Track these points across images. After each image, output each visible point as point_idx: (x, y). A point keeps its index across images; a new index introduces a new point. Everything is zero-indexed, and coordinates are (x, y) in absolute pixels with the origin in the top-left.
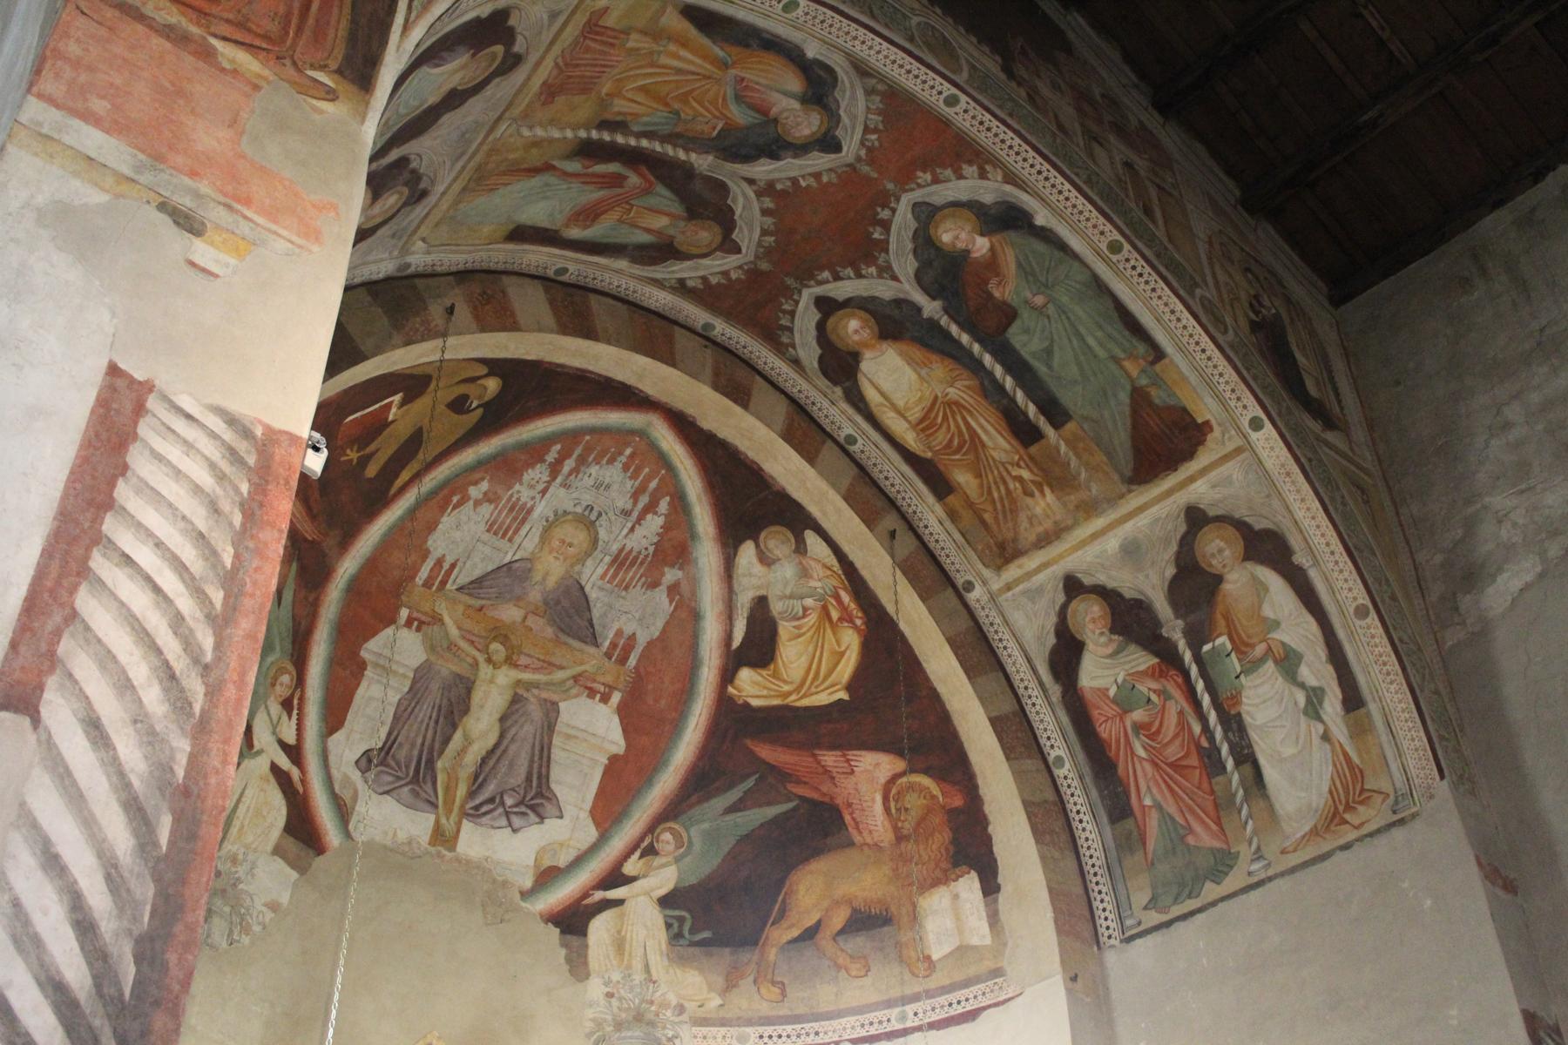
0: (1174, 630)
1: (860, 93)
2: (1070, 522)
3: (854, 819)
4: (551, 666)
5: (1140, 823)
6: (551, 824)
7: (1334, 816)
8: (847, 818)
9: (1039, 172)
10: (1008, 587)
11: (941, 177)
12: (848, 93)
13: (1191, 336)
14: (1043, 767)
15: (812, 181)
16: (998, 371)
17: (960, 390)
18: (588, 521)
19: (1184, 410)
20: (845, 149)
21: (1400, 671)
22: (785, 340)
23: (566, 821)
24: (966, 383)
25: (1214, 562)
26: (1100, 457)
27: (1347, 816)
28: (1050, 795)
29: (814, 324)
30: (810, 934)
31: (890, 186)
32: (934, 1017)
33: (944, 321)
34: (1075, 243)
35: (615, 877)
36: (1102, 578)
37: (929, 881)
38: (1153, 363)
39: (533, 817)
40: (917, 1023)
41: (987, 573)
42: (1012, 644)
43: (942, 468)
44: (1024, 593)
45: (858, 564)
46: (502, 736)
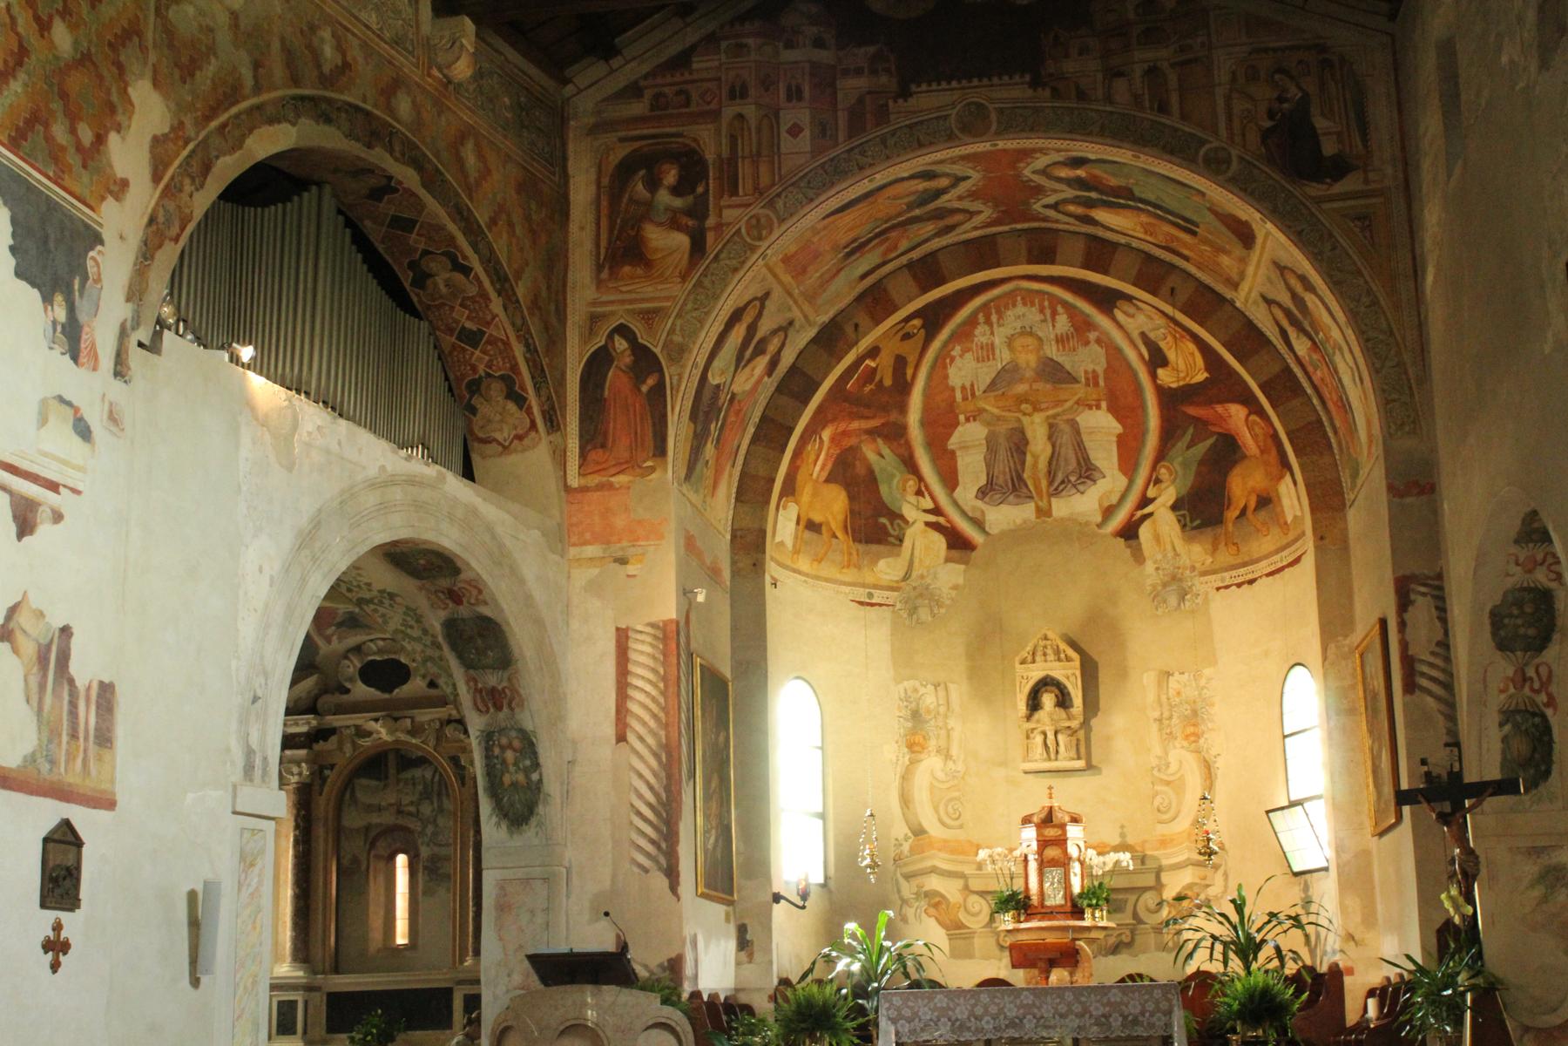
4: (1059, 403)
6: (1101, 483)
17: (1144, 218)
18: (1027, 332)
23: (1108, 479)
30: (1243, 512)
35: (1145, 501)
39: (1089, 482)
41: (1234, 294)
46: (1054, 446)
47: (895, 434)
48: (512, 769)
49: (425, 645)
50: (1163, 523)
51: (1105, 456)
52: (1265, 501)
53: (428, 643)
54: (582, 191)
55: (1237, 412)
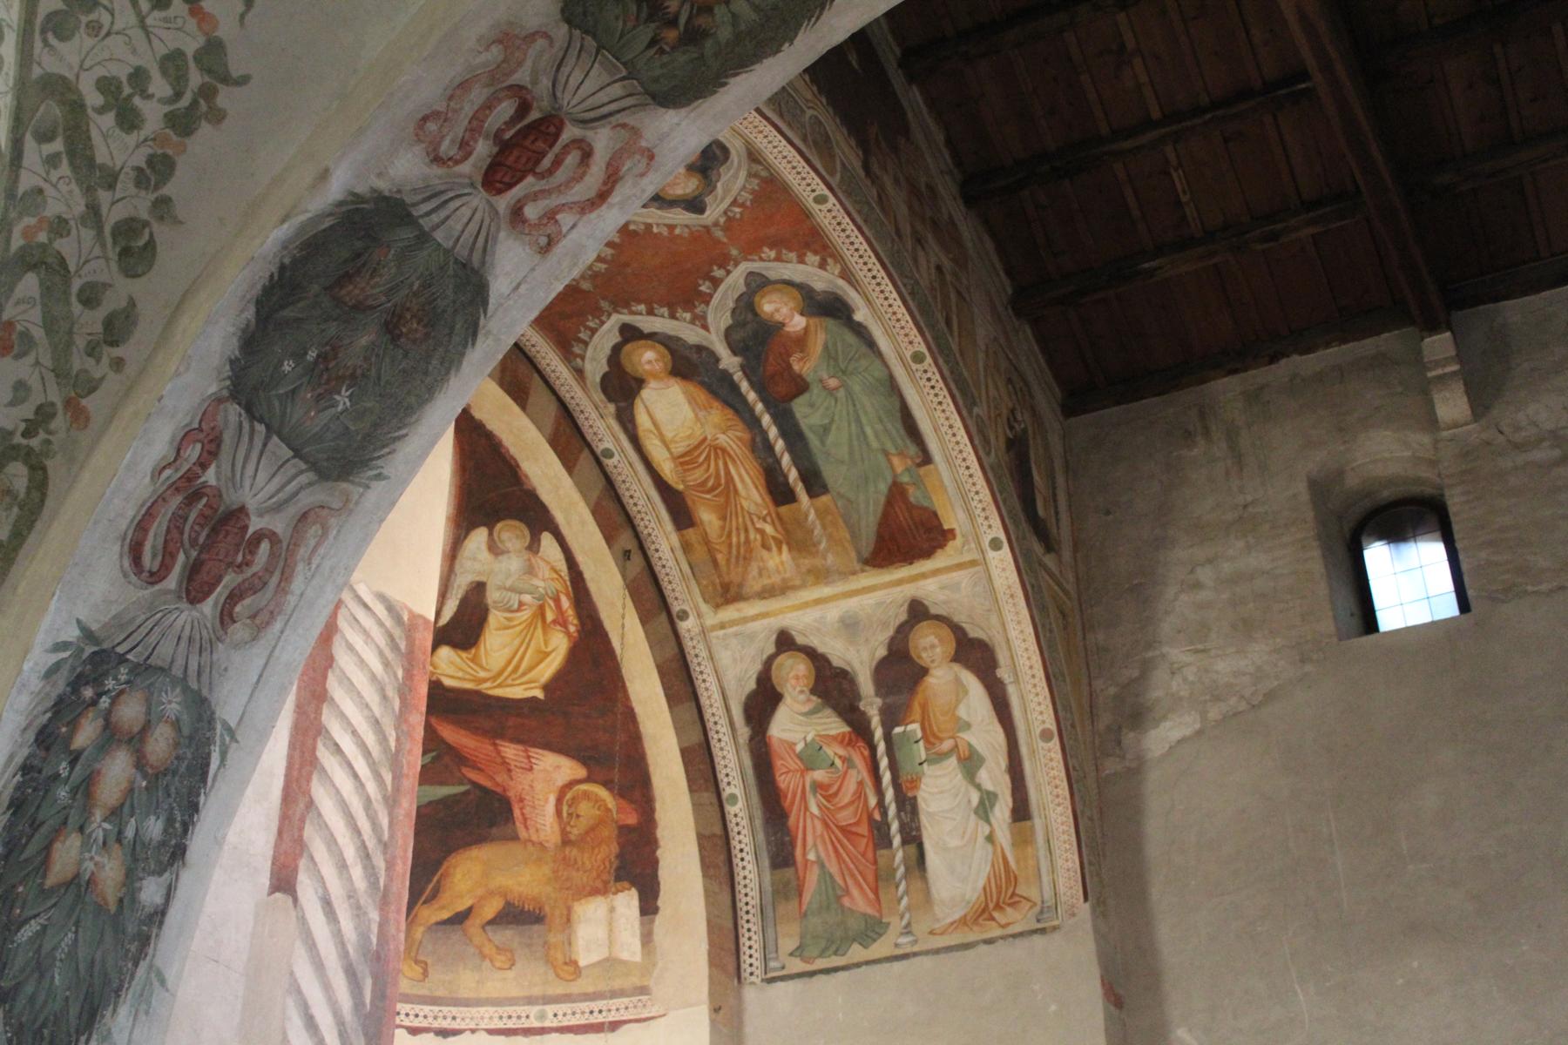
0: (871, 706)
1: (743, 174)
2: (798, 582)
3: (523, 814)
5: (801, 874)
7: (984, 911)
8: (517, 812)
9: (874, 277)
10: (722, 626)
11: (784, 257)
12: (732, 172)
13: (961, 452)
14: (715, 801)
15: (665, 232)
16: (773, 432)
17: (732, 438)
19: (935, 514)
20: (707, 213)
21: (1068, 796)
22: (577, 350)
24: (739, 434)
25: (924, 655)
26: (844, 534)
27: (996, 915)
28: (718, 830)
29: (611, 344)
30: (460, 919)
31: (734, 252)
32: (574, 1021)
33: (738, 376)
34: (883, 343)
36: (815, 642)
37: (588, 888)
38: (919, 465)
40: (555, 1024)
41: (704, 607)
42: (712, 681)
43: (690, 503)
44: (736, 635)
45: (587, 575)
48: (99, 825)
49: (93, 213)
53: (113, 216)
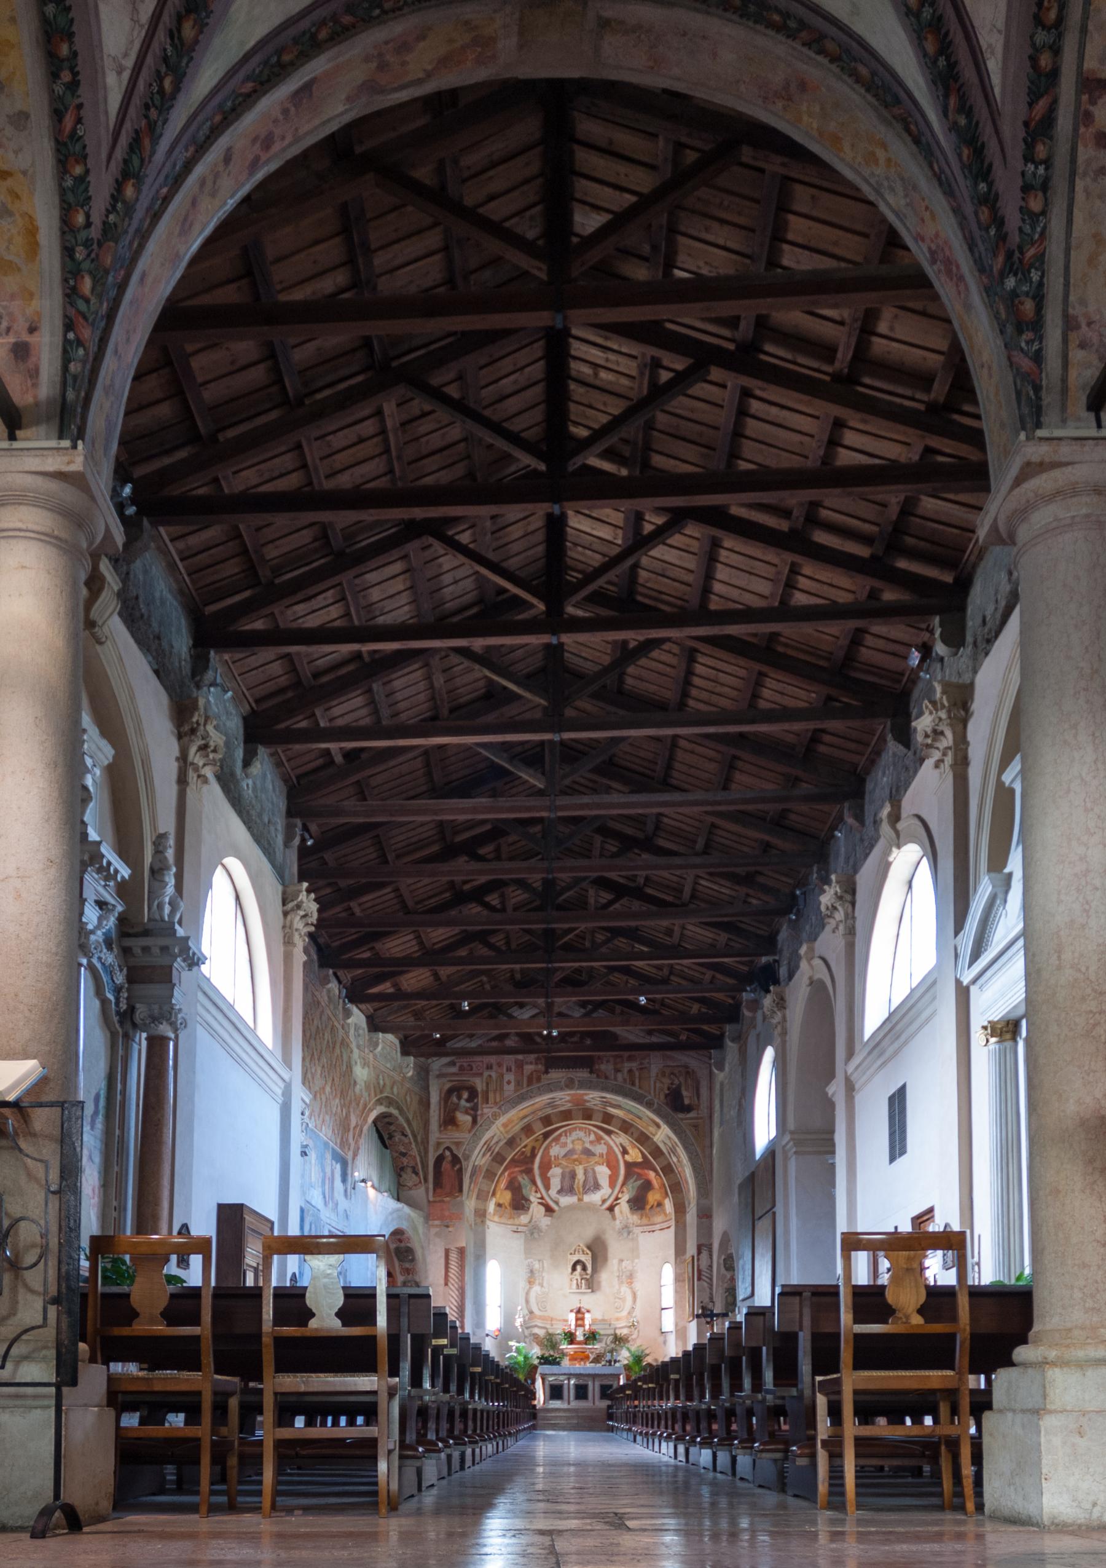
35: (617, 1199)
47: (529, 1172)
50: (623, 1207)
51: (604, 1182)
52: (660, 1204)
54: (435, 1098)
55: (652, 1175)
